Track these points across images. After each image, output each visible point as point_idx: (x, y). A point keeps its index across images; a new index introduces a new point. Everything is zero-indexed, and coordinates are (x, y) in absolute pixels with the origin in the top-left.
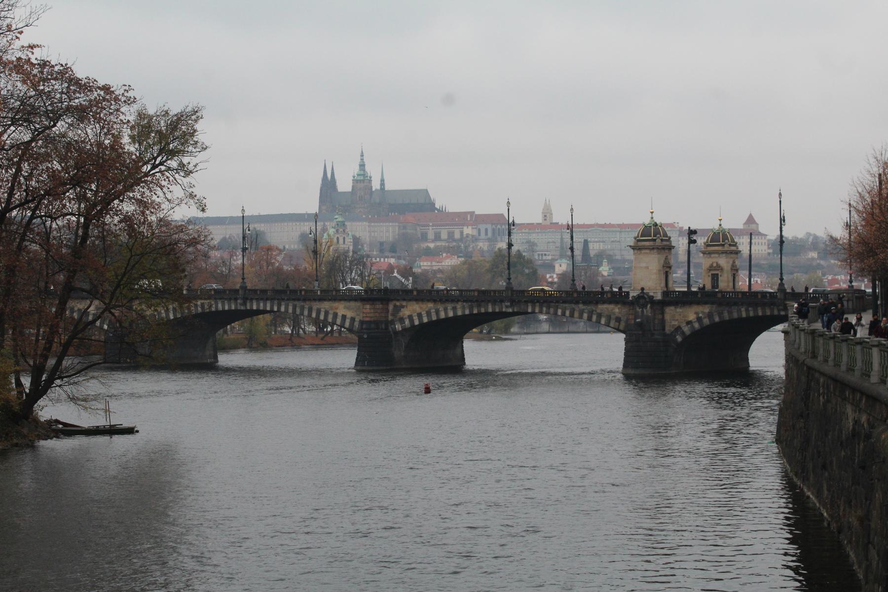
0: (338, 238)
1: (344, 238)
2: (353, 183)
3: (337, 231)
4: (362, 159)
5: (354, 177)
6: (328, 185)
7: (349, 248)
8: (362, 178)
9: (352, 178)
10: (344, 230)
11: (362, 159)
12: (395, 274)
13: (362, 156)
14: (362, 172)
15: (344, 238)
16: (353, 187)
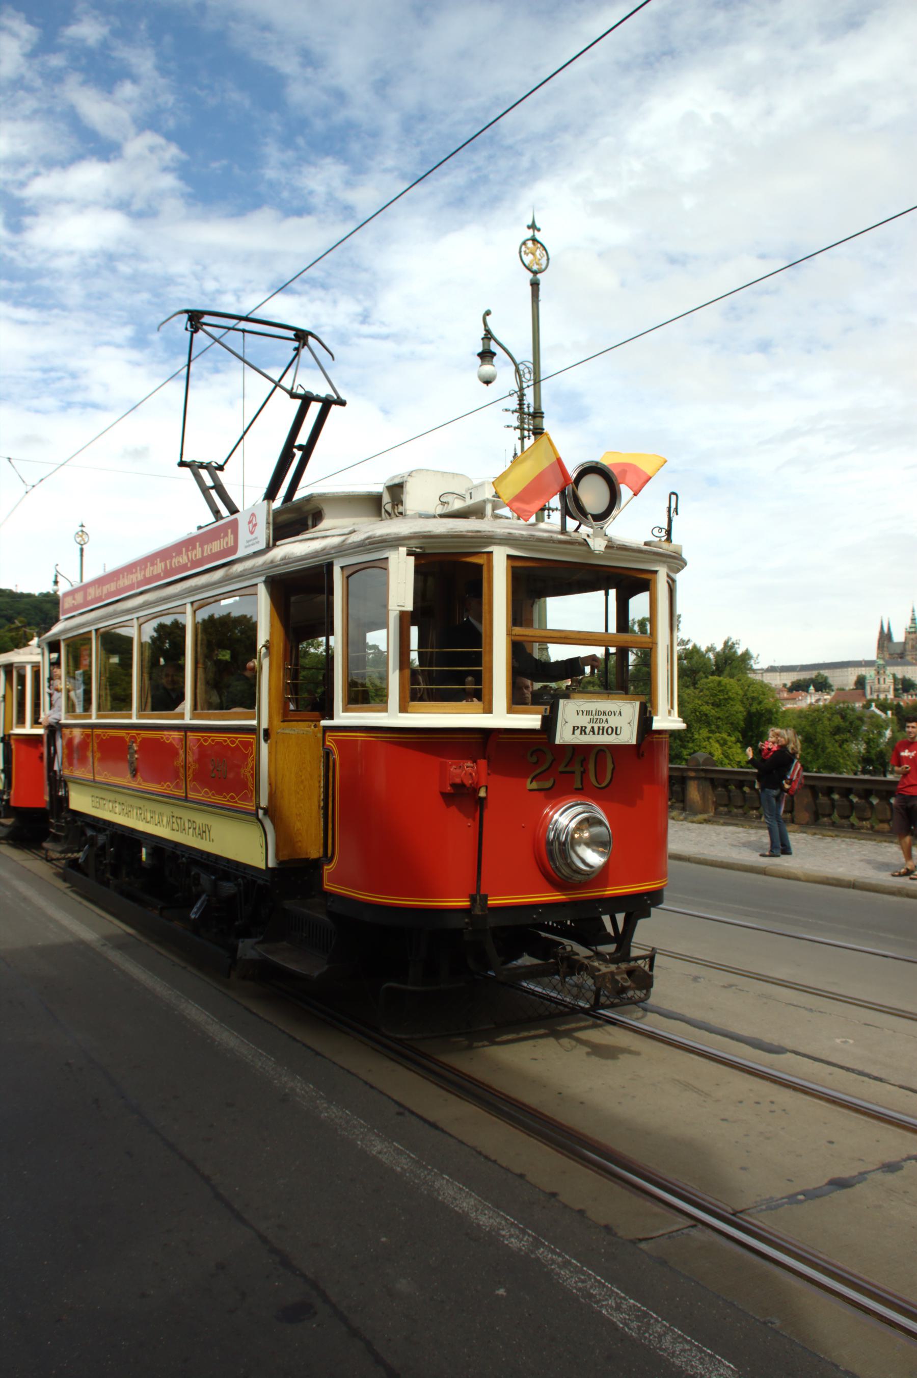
0: (879, 679)
1: (884, 679)
2: (906, 634)
3: (878, 673)
4: (913, 615)
5: (906, 629)
6: (885, 638)
7: (889, 687)
8: (913, 630)
9: (904, 630)
10: (884, 672)
11: (913, 615)
12: (873, 708)
13: (913, 611)
14: (913, 625)
15: (884, 679)
16: (906, 638)
